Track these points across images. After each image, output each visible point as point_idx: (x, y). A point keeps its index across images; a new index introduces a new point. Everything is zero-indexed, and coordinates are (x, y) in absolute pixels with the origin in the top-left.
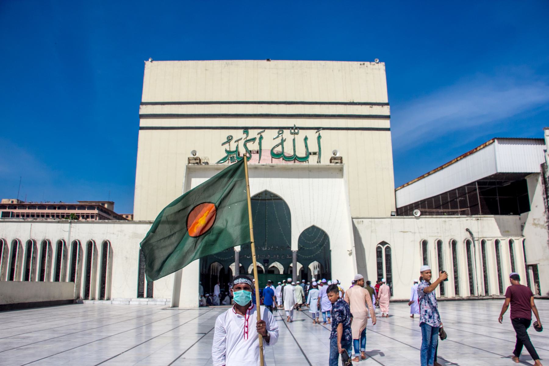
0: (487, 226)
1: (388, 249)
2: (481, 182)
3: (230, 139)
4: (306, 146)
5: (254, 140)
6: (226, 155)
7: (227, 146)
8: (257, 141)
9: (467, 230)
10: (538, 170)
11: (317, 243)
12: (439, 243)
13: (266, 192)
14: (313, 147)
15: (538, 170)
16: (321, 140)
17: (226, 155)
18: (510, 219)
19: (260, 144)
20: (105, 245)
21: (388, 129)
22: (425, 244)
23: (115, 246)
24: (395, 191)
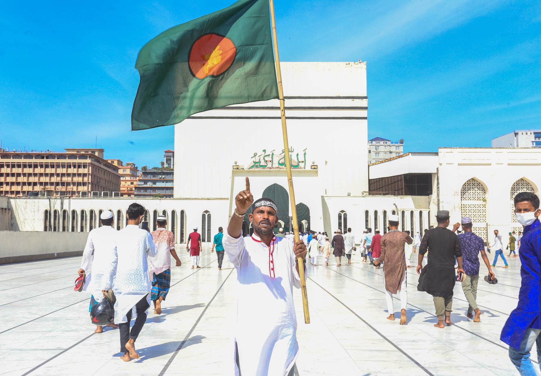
0: (407, 203)
1: (345, 215)
2: (405, 175)
3: (255, 155)
4: (298, 159)
5: (269, 155)
6: (253, 164)
7: (254, 159)
8: (271, 156)
9: (394, 204)
10: (436, 172)
11: (303, 212)
12: (376, 212)
13: (275, 185)
14: (301, 159)
15: (436, 172)
16: (306, 155)
17: (253, 164)
18: (422, 199)
19: (272, 158)
20: (182, 212)
21: (365, 118)
22: (367, 212)
23: (187, 213)
24: (369, 166)
